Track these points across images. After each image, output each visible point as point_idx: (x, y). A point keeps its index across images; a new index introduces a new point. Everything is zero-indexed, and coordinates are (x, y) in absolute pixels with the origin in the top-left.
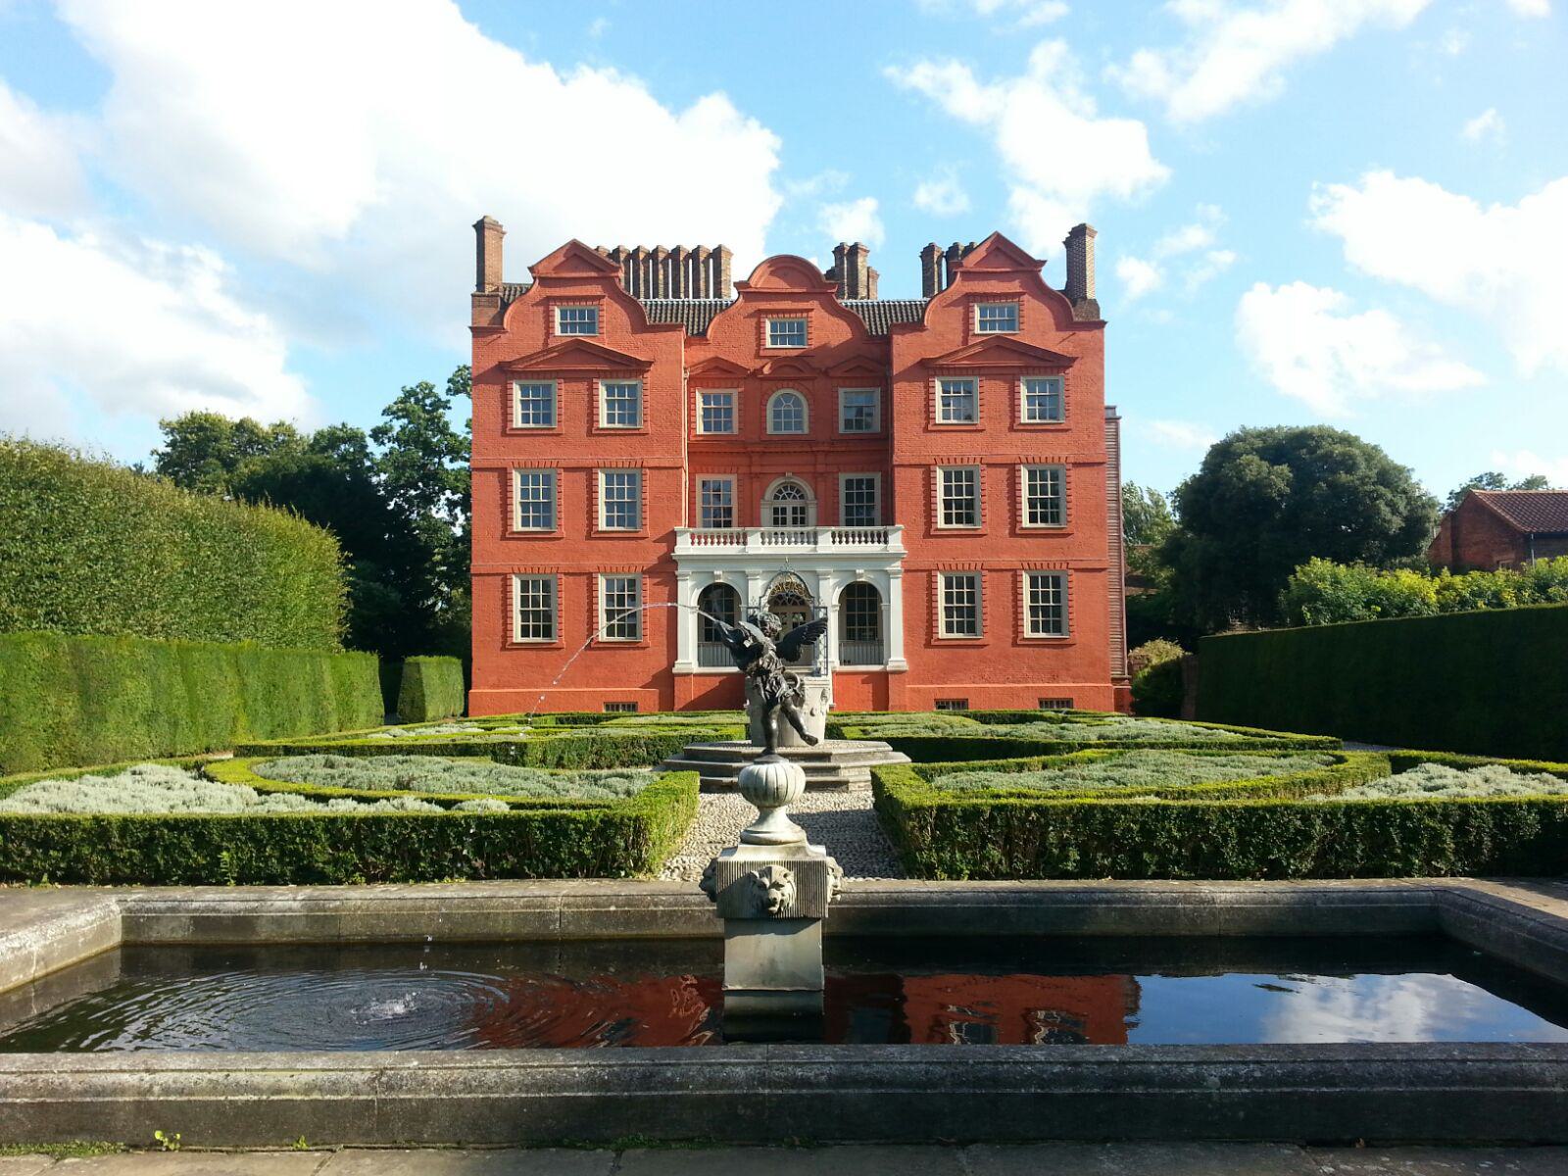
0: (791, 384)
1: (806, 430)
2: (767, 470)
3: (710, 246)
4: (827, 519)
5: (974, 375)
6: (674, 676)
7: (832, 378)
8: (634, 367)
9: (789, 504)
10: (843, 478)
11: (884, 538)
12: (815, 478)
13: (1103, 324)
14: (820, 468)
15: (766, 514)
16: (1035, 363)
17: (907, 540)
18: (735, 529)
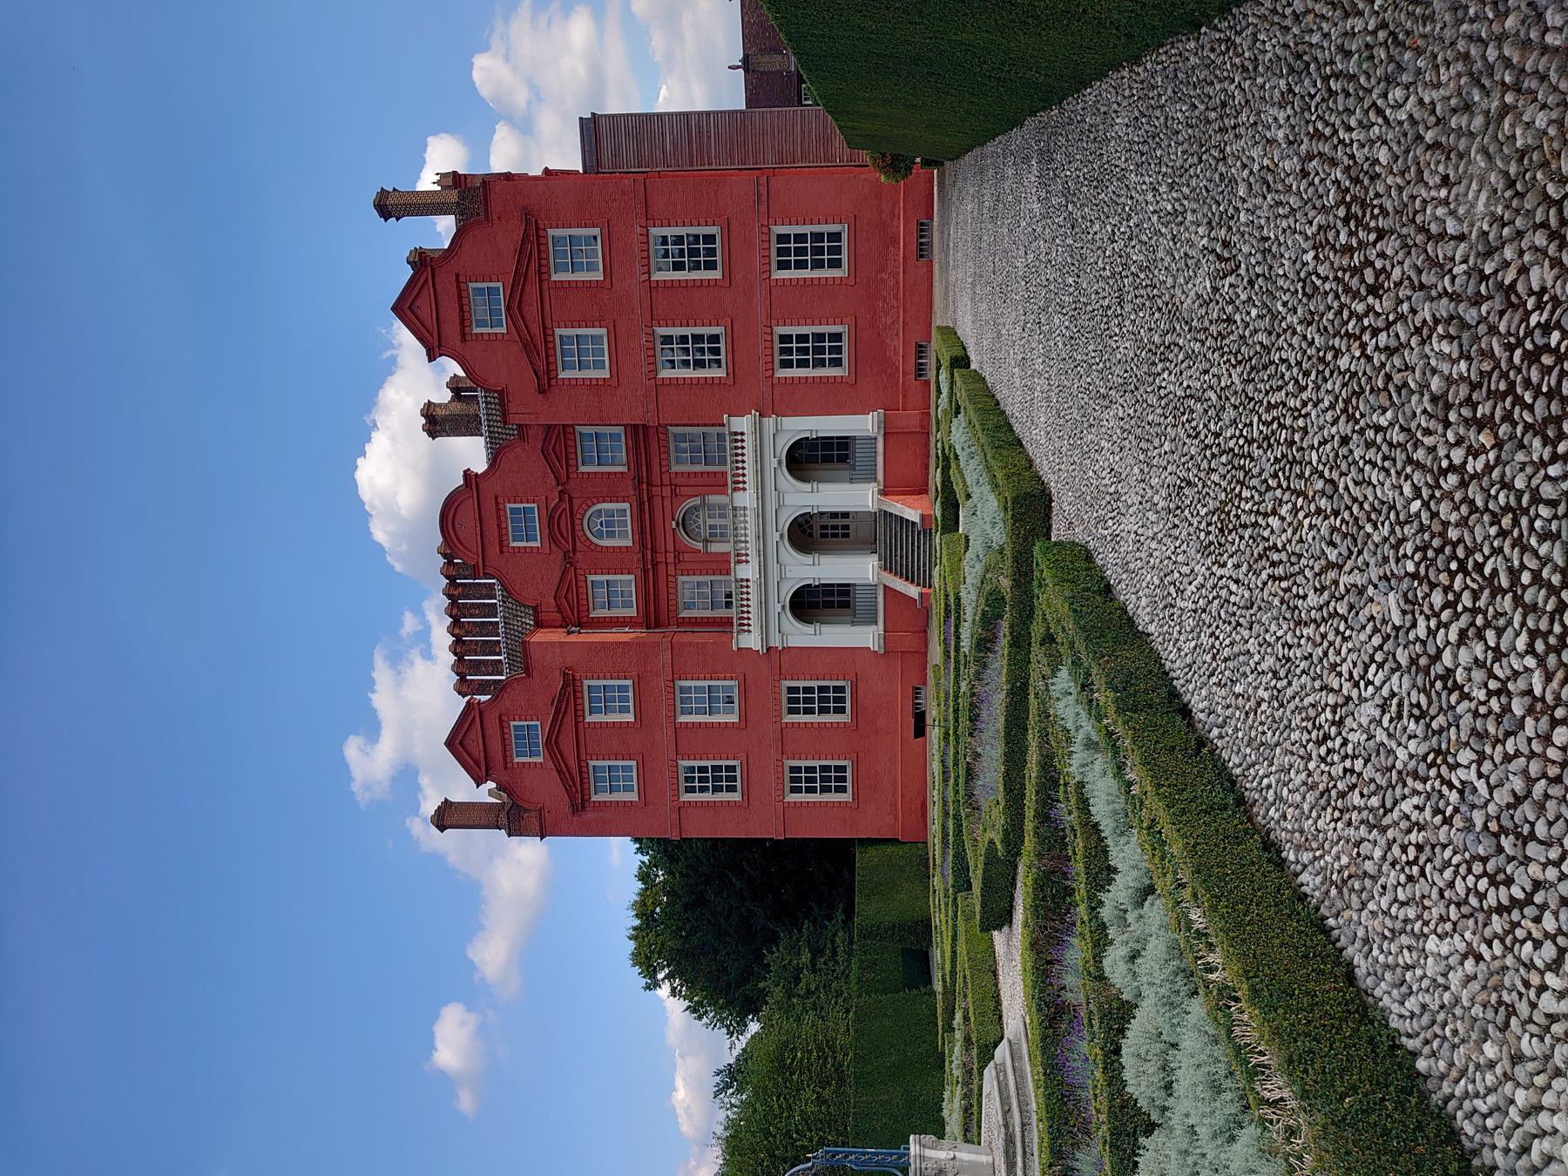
0: (577, 522)
1: (626, 506)
2: (670, 547)
5: (553, 335)
7: (568, 478)
14: (667, 492)
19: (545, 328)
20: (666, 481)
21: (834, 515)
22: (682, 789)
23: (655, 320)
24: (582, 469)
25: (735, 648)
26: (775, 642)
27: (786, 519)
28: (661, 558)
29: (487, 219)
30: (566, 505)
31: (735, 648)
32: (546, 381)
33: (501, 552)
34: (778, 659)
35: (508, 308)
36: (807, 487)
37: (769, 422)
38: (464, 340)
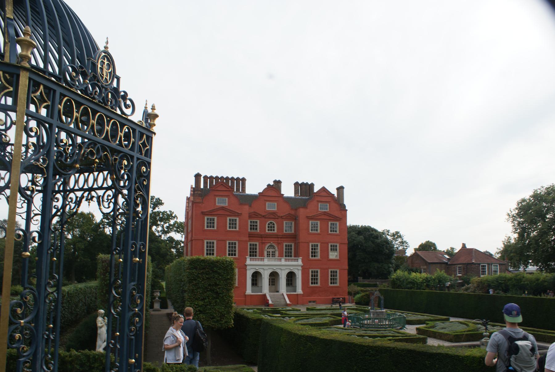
0: (272, 219)
3: (241, 177)
4: (281, 255)
6: (245, 295)
8: (237, 214)
9: (271, 250)
10: (284, 244)
11: (297, 260)
12: (278, 244)
13: (347, 210)
15: (266, 253)
16: (333, 219)
17: (303, 261)
18: (258, 257)
19: (320, 219)
20: (282, 242)
21: (269, 282)
22: (208, 241)
23: (322, 243)
24: (285, 222)
25: (247, 257)
26: (248, 267)
27: (278, 271)
28: (263, 239)
29: (341, 210)
30: (277, 217)
31: (247, 257)
32: (309, 218)
33: (265, 200)
34: (244, 268)
35: (325, 212)
36: (286, 277)
37: (300, 268)
38: (318, 201)
